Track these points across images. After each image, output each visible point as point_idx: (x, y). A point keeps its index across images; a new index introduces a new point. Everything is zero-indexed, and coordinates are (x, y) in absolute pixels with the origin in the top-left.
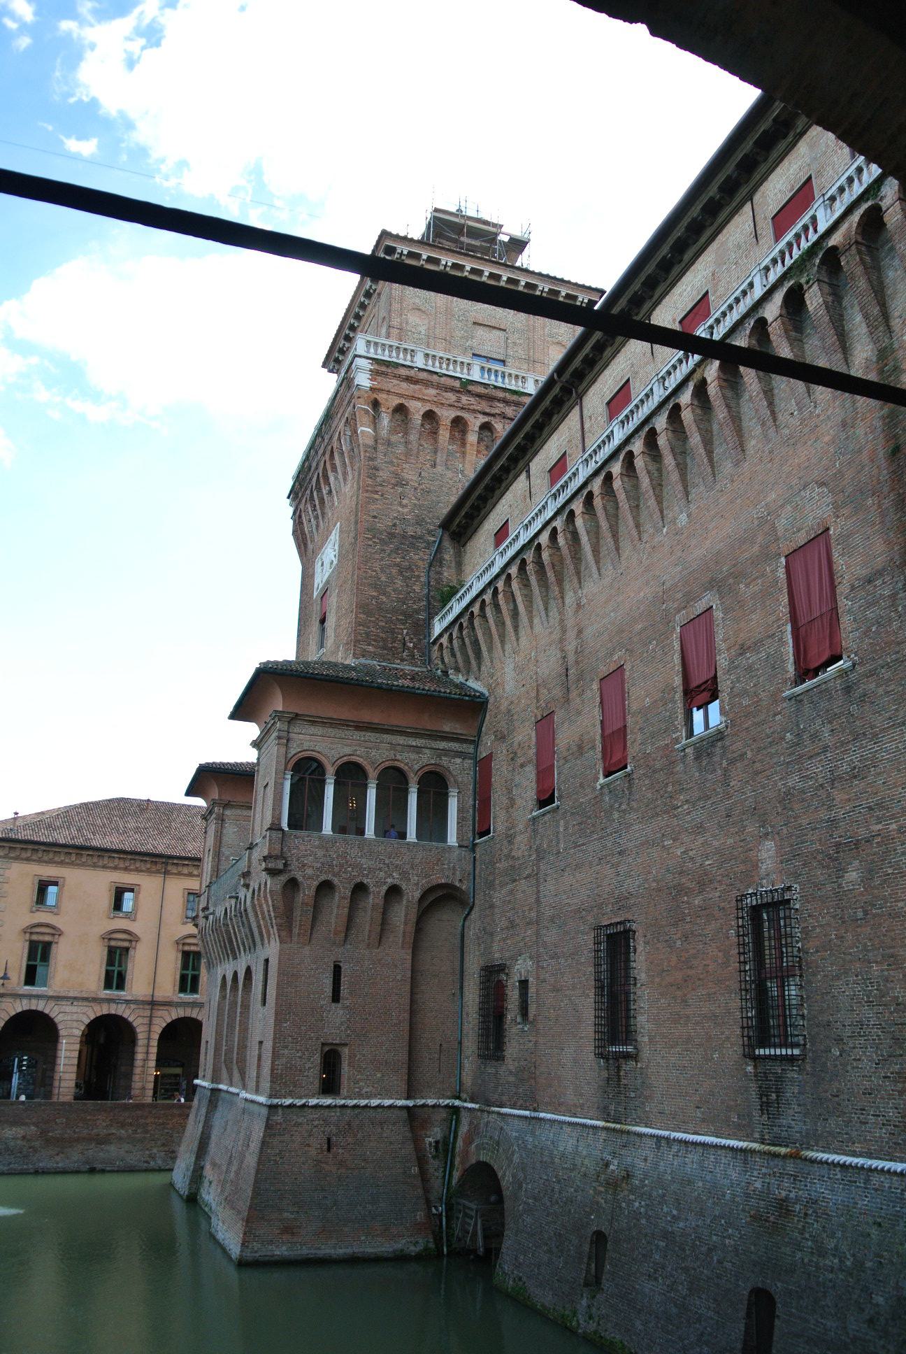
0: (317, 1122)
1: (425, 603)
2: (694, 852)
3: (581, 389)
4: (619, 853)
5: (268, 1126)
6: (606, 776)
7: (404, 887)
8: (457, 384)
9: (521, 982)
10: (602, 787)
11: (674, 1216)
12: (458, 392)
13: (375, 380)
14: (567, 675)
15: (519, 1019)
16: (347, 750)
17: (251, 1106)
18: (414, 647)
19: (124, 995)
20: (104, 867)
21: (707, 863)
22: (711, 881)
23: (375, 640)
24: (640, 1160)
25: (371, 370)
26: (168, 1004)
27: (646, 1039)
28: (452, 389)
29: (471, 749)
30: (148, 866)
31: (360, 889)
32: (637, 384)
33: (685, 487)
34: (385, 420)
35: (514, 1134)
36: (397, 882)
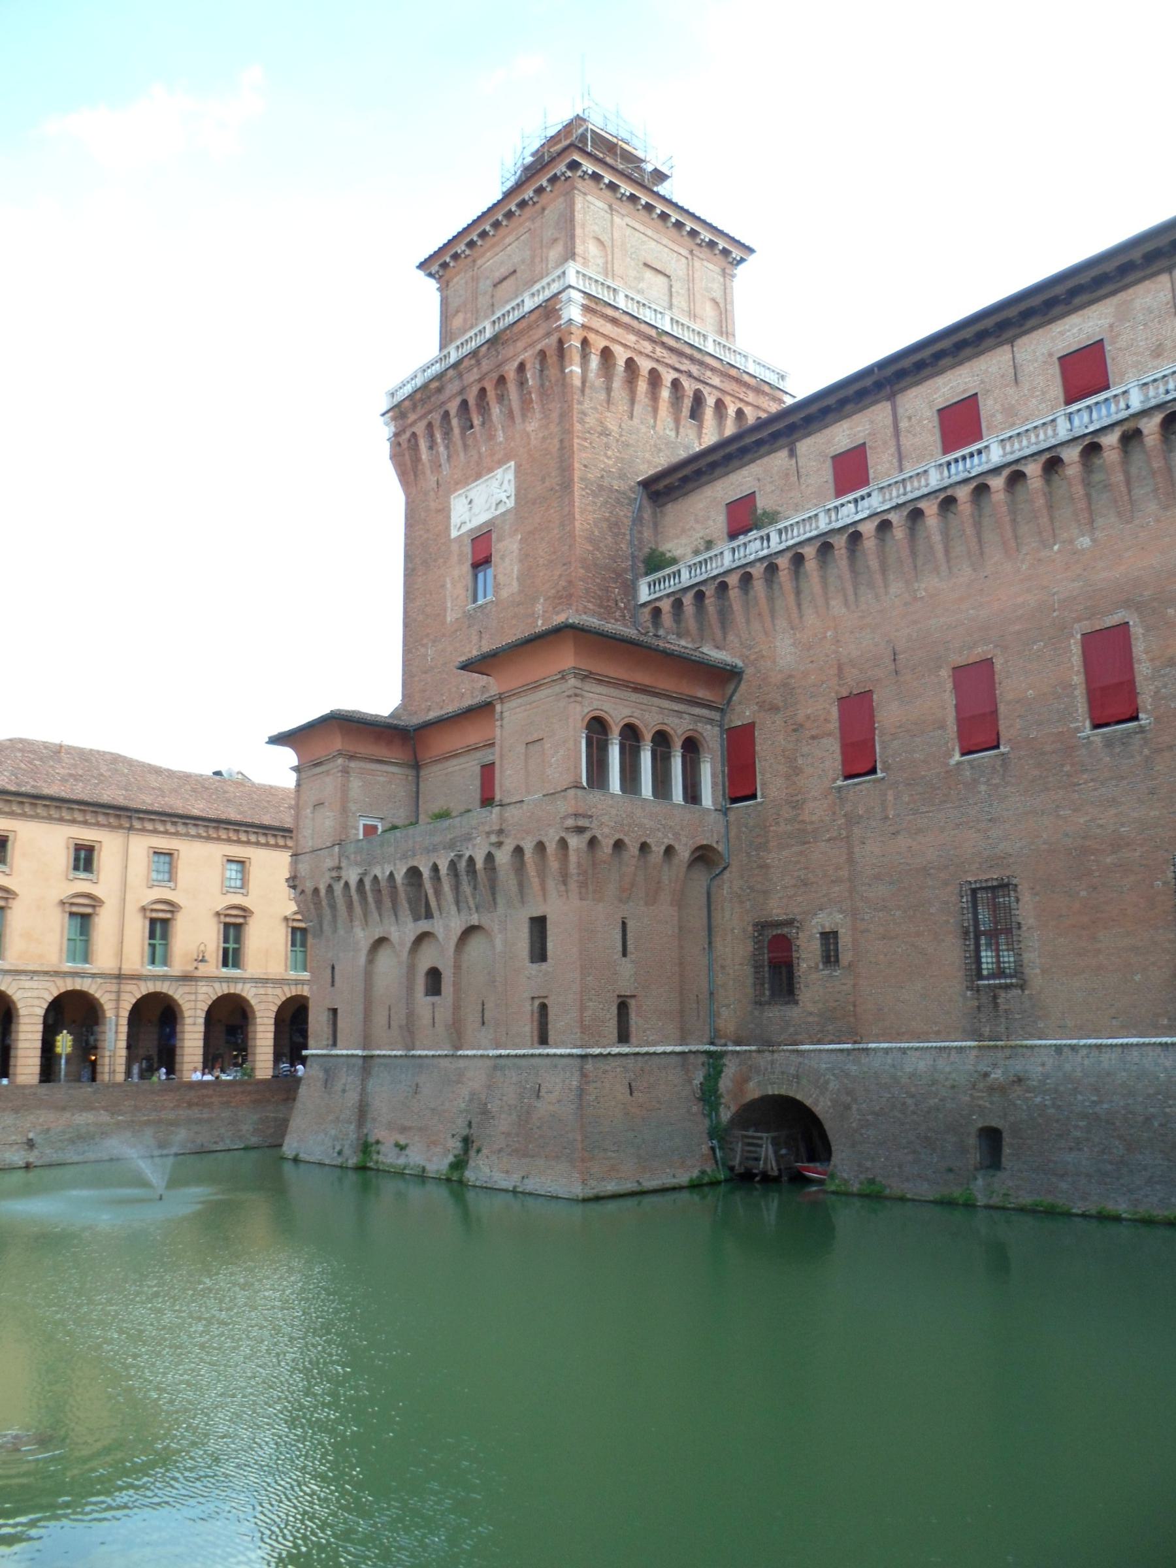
0: (618, 1070)
1: (630, 563)
2: (1104, 821)
3: (896, 387)
4: (990, 820)
5: (584, 1075)
6: (963, 754)
7: (677, 847)
8: (653, 333)
9: (825, 935)
10: (959, 763)
11: (1093, 1102)
12: (655, 342)
13: (585, 316)
14: (895, 660)
15: (821, 966)
16: (627, 712)
17: (502, 1061)
18: (625, 608)
19: (91, 969)
20: (61, 820)
21: (1123, 829)
22: (1128, 844)
23: (593, 597)
24: (1034, 1068)
25: (583, 305)
26: (137, 977)
27: (1038, 971)
28: (649, 338)
29: (716, 716)
30: (112, 820)
31: (644, 847)
32: (990, 402)
33: (1091, 514)
34: (595, 361)
35: (824, 1066)
36: (672, 843)
